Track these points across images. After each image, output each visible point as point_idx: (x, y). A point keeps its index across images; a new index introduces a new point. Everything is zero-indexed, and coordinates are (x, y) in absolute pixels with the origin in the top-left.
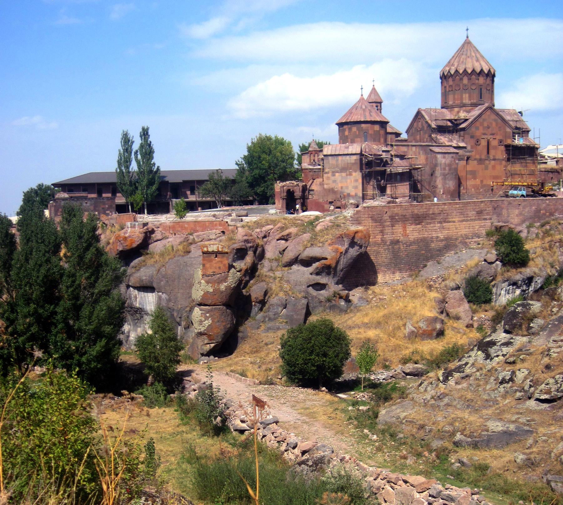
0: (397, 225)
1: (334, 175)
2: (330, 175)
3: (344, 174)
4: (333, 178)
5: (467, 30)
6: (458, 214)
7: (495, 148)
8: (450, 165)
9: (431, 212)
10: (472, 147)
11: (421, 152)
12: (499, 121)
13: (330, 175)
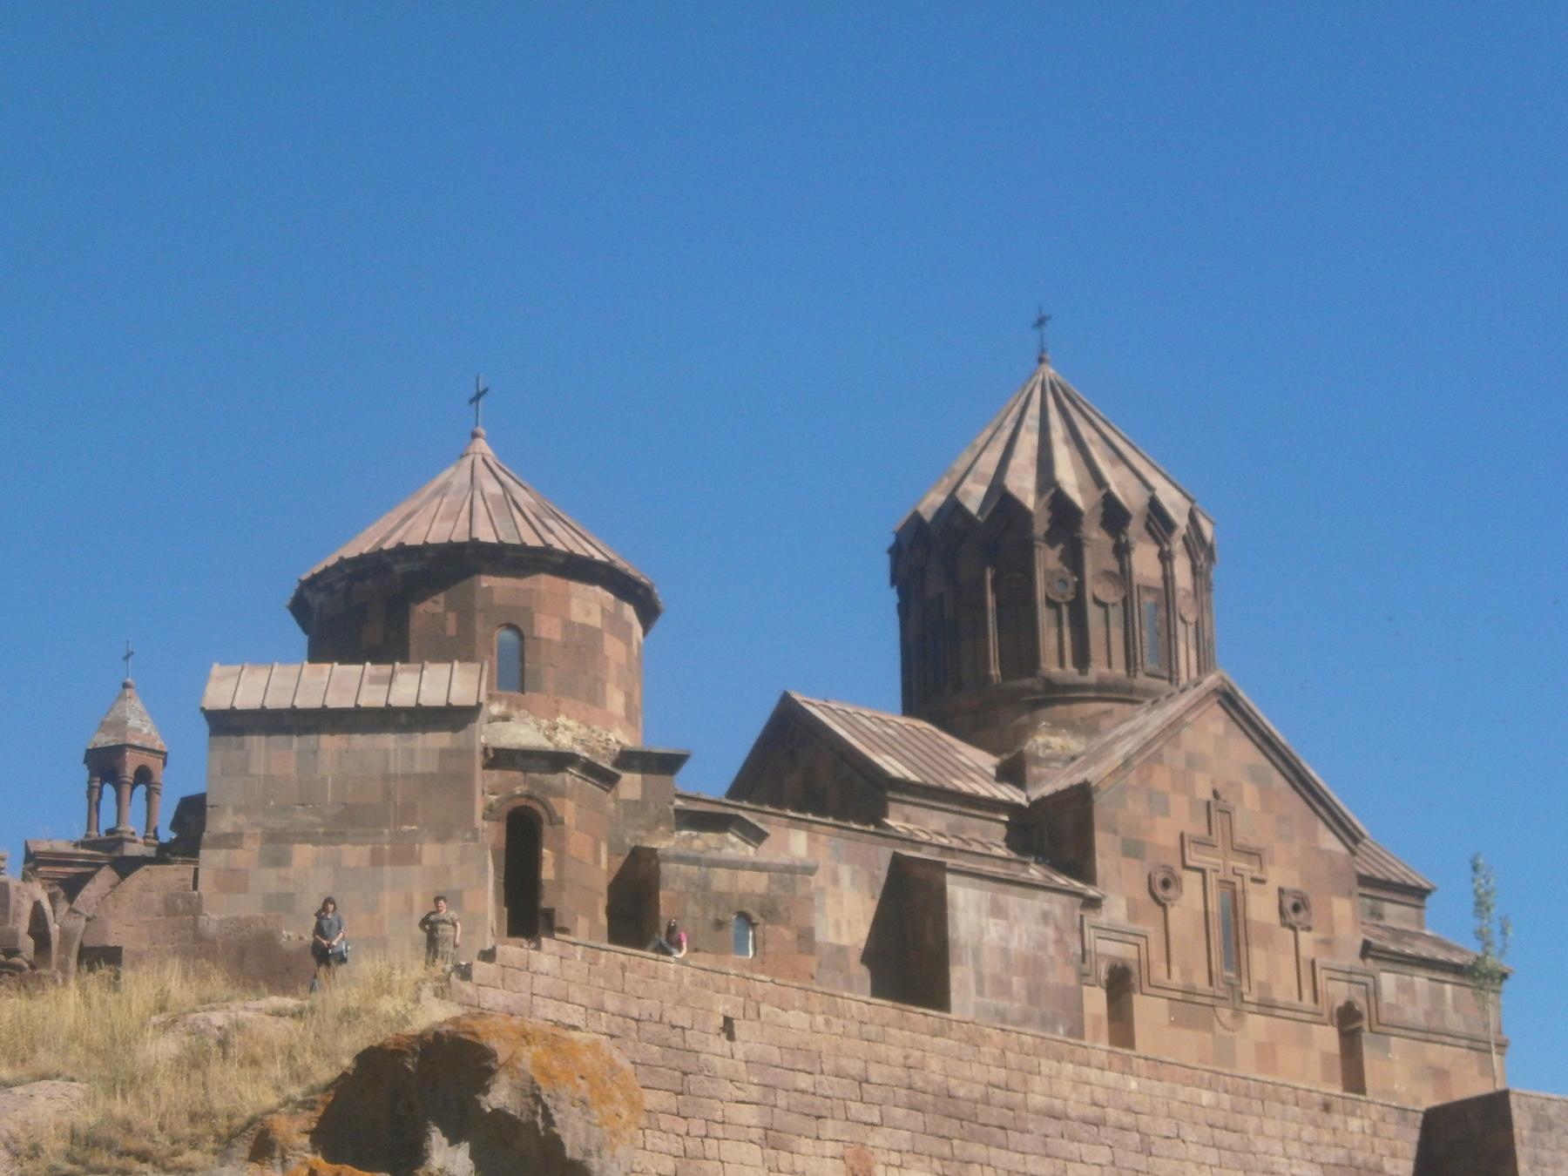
0: (806, 1145)
1: (279, 860)
2: (246, 855)
3: (354, 854)
4: (269, 879)
5: (1041, 322)
6: (1211, 1156)
8: (1033, 966)
9: (1037, 1100)
10: (1133, 914)
11: (845, 872)
12: (1278, 780)
13: (246, 855)
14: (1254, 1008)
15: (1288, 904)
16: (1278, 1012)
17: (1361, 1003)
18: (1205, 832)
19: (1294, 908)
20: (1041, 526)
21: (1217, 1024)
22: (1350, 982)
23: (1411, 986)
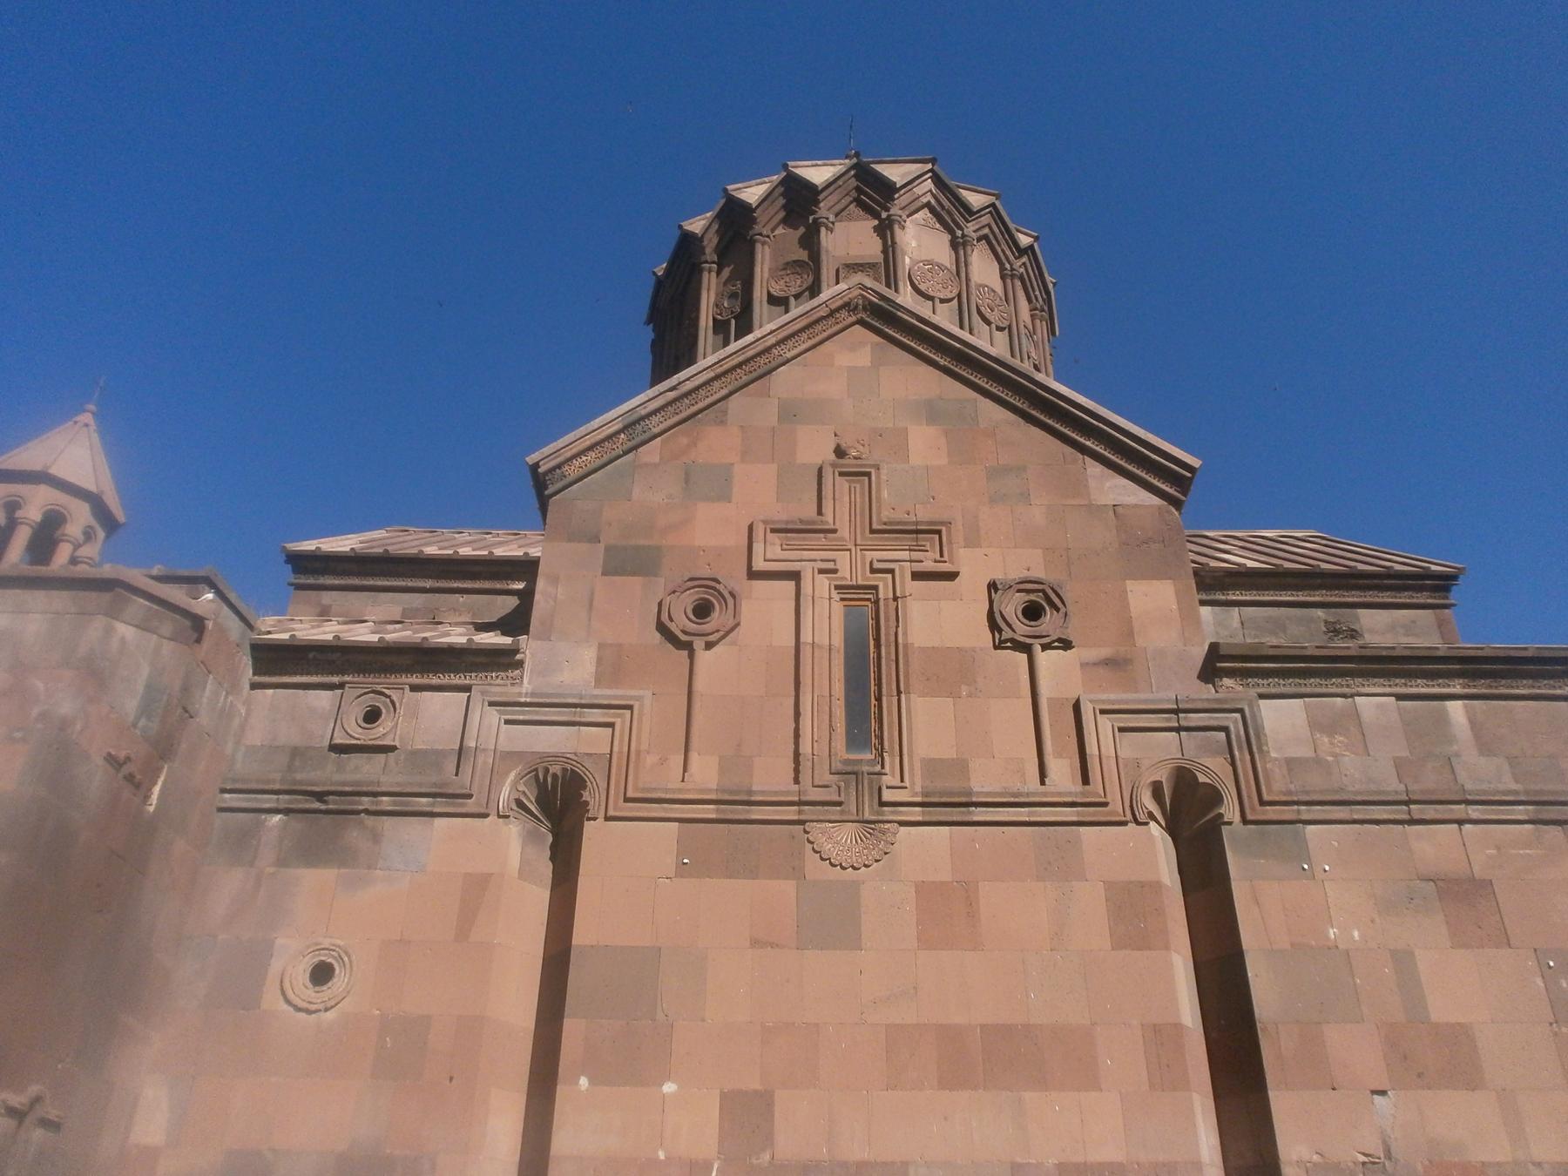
7: (953, 673)
12: (992, 413)
14: (916, 814)
15: (1011, 606)
16: (980, 814)
17: (1213, 768)
18: (810, 511)
19: (1030, 615)
20: (711, 243)
21: (811, 859)
22: (1178, 730)
23: (1356, 714)
